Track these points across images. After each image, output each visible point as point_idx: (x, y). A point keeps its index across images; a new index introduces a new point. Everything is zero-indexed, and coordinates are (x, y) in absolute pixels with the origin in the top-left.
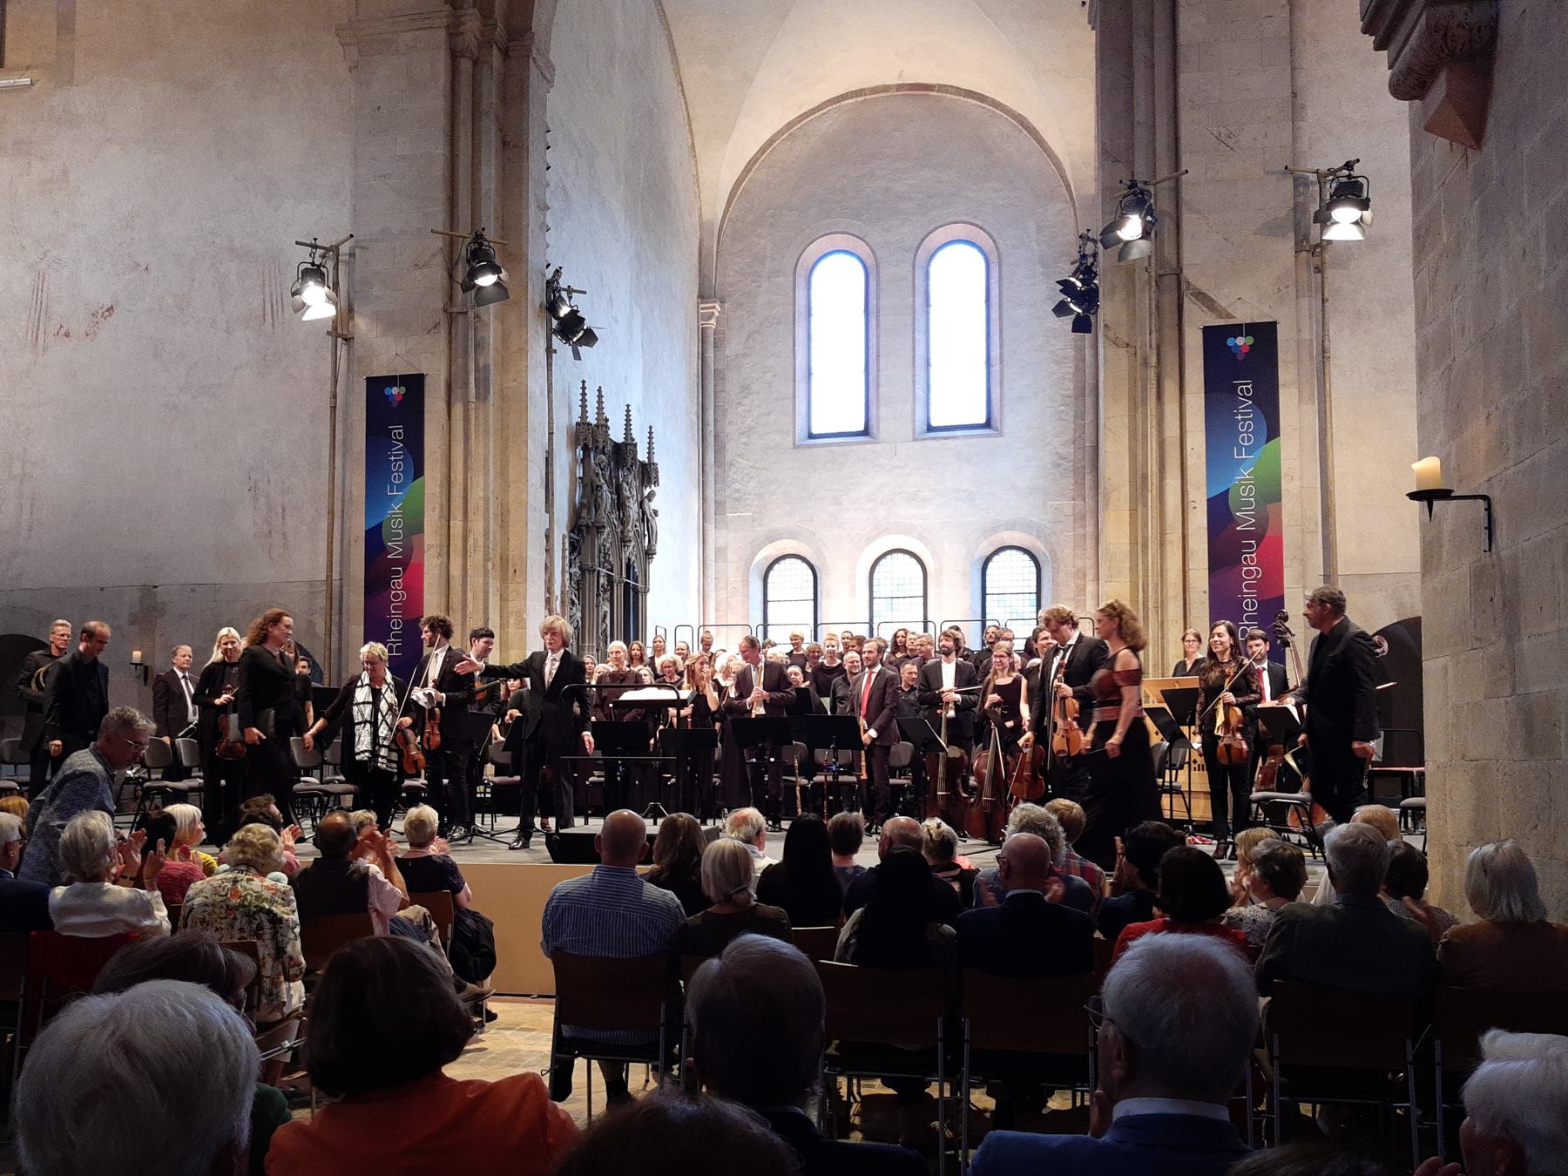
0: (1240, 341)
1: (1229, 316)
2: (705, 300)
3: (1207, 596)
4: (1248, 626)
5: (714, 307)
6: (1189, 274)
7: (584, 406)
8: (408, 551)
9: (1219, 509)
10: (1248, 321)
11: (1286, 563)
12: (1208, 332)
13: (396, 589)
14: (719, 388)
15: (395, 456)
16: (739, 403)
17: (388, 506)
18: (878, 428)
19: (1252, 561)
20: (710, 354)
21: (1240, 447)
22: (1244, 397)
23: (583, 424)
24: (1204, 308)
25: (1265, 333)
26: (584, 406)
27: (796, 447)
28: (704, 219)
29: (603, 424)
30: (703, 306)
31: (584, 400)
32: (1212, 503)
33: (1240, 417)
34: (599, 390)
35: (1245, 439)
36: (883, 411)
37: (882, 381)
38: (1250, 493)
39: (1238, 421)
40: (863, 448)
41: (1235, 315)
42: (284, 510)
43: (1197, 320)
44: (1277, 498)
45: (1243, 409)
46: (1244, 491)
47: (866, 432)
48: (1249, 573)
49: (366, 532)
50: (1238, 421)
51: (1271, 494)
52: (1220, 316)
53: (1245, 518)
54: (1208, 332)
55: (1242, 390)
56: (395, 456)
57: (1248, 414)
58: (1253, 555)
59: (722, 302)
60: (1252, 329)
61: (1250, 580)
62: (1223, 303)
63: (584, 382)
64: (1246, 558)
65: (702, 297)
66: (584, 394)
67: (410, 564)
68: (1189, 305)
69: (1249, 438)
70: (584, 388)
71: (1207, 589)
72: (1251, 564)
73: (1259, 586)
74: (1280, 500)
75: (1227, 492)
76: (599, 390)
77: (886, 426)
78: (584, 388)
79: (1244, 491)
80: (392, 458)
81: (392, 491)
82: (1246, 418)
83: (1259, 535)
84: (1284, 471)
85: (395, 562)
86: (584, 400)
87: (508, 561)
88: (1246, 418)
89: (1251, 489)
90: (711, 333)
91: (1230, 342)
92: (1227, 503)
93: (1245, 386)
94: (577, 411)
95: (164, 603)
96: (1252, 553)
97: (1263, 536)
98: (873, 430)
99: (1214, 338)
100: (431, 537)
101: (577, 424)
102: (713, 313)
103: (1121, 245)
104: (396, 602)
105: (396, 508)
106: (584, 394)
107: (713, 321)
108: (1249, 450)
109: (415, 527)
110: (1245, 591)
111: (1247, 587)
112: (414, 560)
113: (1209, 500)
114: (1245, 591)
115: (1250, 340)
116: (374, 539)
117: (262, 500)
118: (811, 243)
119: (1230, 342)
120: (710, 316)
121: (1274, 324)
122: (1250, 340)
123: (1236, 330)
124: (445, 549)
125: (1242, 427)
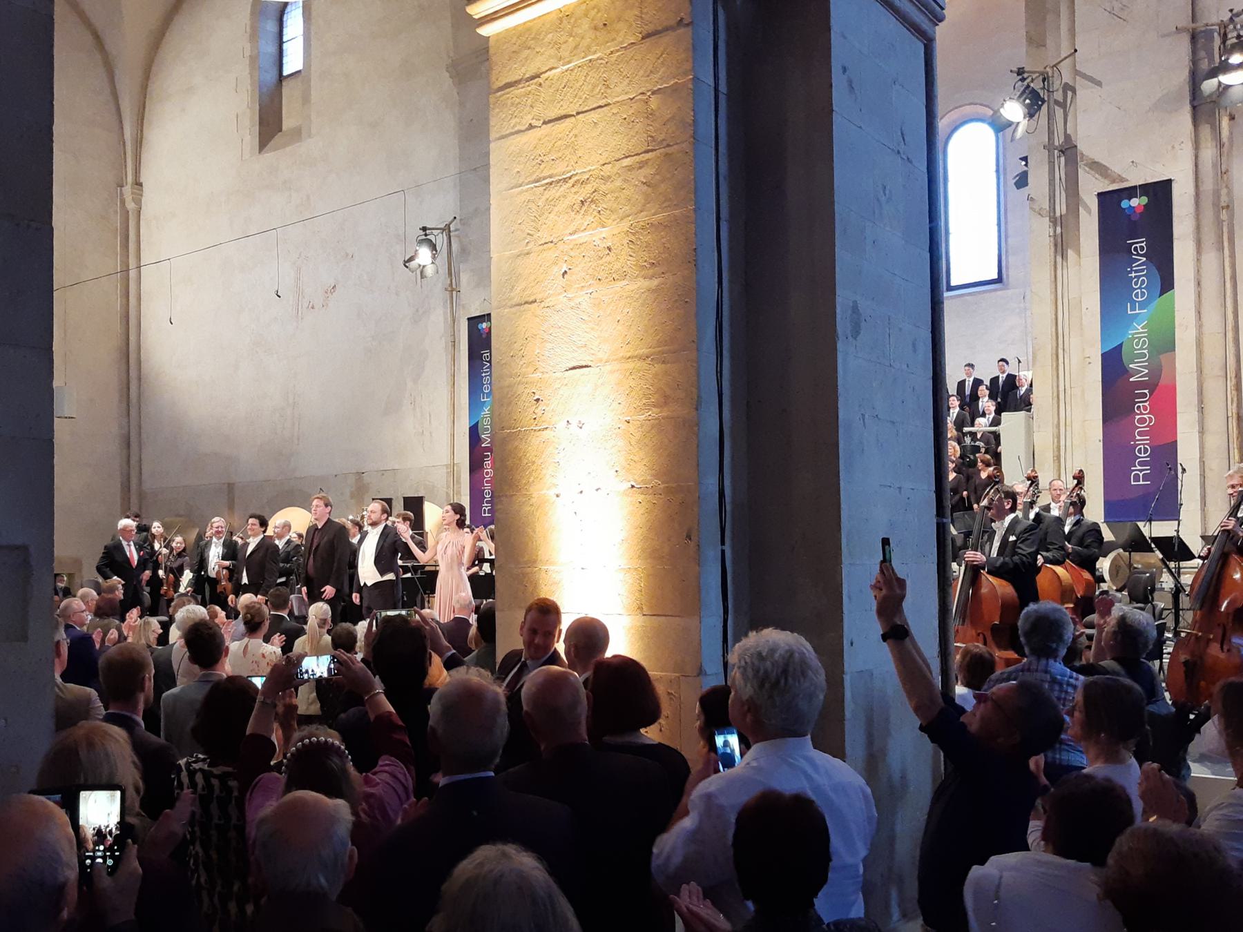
0: (1135, 202)
1: (1122, 180)
3: (1101, 443)
4: (1141, 471)
6: (1082, 147)
9: (1113, 364)
10: (1141, 182)
19: (1146, 410)
21: (1133, 303)
22: (1138, 254)
24: (1097, 176)
25: (1160, 192)
32: (1106, 357)
33: (1133, 275)
37: (1010, 232)
38: (1142, 345)
39: (1132, 278)
40: (997, 295)
42: (430, 416)
43: (1091, 187)
44: (1170, 346)
45: (1135, 267)
47: (999, 280)
48: (1142, 421)
49: (470, 428)
51: (1165, 344)
52: (1113, 181)
53: (1138, 369)
54: (1100, 195)
55: (1136, 249)
56: (485, 372)
57: (1143, 270)
58: (1146, 404)
60: (1146, 189)
61: (1143, 427)
62: (1116, 168)
64: (1139, 407)
68: (1084, 176)
69: (1143, 294)
71: (1101, 439)
72: (1144, 414)
73: (1152, 432)
75: (1122, 343)
77: (1012, 275)
80: (484, 375)
81: (483, 398)
82: (1140, 273)
83: (1152, 385)
85: (487, 449)
88: (1140, 273)
92: (1122, 360)
97: (1157, 385)
99: (1109, 201)
103: (1015, 124)
105: (486, 410)
108: (1143, 305)
110: (1138, 438)
111: (1140, 434)
114: (1138, 438)
115: (1144, 200)
116: (474, 434)
119: (1125, 204)
121: (1169, 182)
122: (1144, 200)
123: (1131, 192)
125: (1136, 284)
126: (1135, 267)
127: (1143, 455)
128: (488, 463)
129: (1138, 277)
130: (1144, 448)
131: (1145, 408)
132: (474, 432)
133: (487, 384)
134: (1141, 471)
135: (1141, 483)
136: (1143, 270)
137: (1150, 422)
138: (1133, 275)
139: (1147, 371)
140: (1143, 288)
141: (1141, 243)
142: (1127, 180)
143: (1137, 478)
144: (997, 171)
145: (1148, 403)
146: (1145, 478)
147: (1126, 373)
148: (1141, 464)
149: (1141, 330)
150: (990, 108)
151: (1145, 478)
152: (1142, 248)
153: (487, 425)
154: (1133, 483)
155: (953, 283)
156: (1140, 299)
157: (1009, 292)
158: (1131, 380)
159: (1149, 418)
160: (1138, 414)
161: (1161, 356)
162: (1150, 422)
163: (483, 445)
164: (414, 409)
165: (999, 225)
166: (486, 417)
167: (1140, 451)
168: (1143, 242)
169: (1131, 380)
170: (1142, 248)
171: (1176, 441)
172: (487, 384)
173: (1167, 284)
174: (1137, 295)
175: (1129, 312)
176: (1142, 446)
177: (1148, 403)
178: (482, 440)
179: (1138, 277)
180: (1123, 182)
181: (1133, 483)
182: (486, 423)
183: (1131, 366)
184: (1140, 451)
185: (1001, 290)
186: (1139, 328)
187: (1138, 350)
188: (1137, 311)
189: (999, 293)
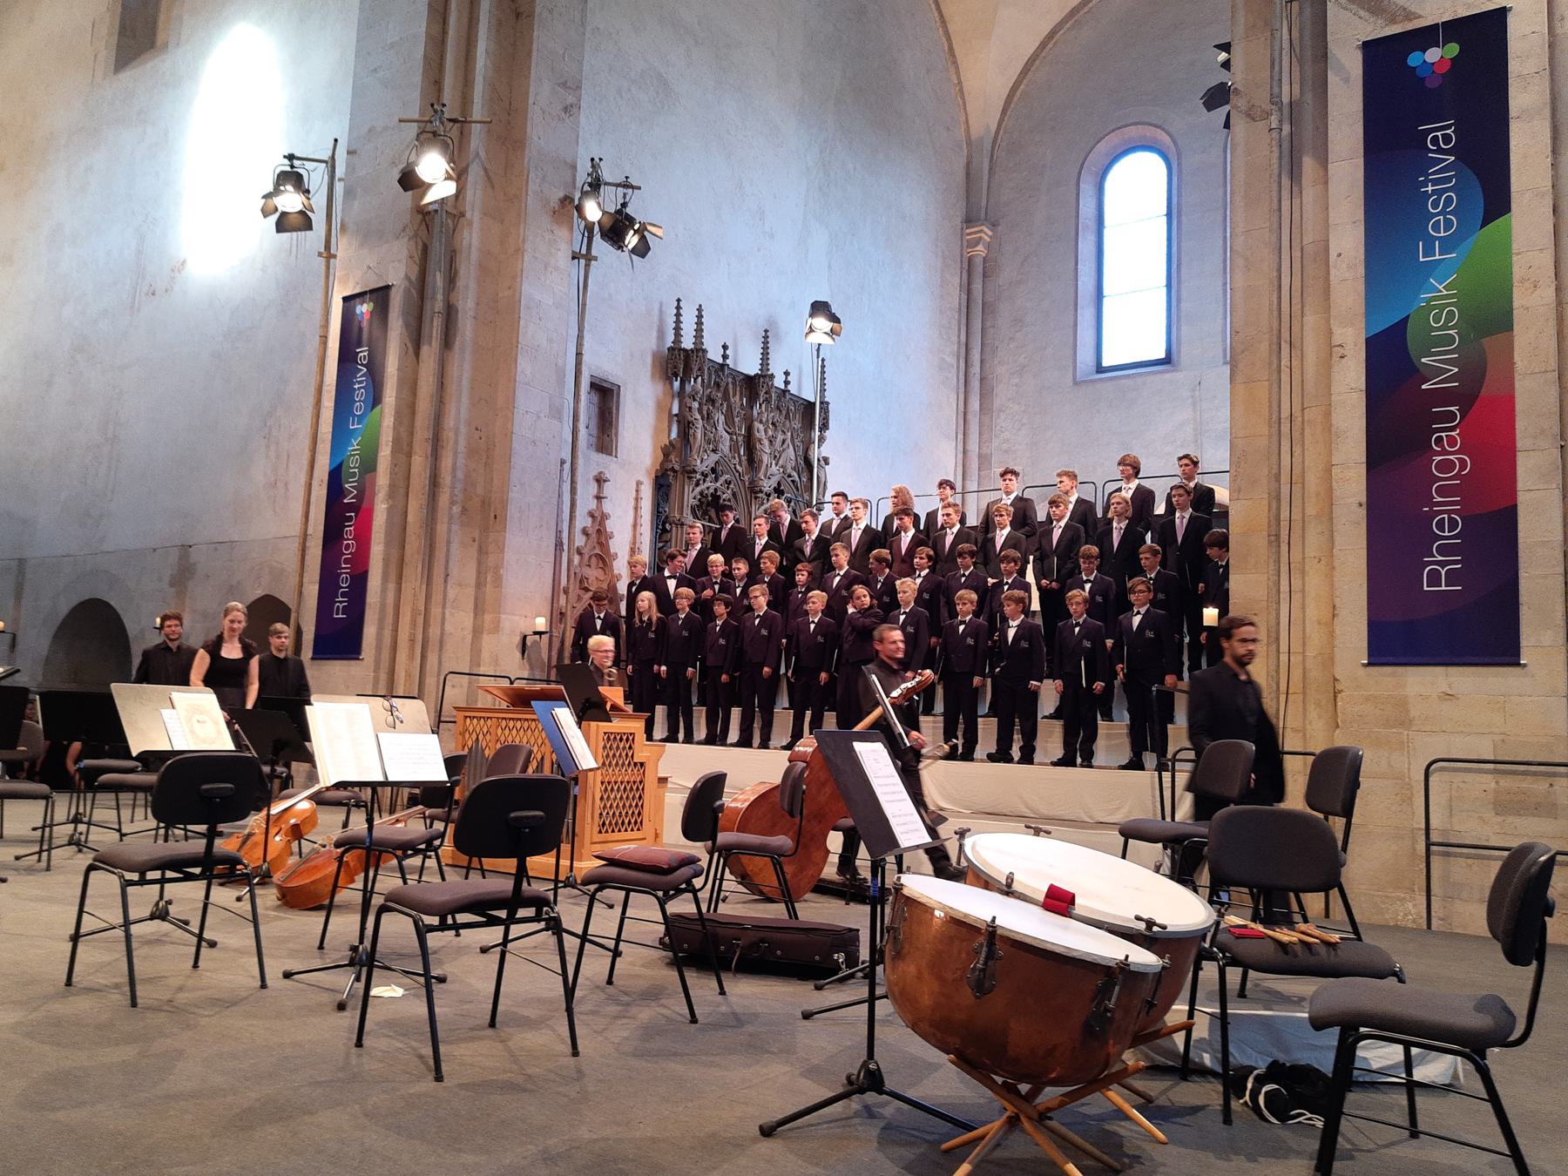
0: (1433, 55)
1: (1409, 16)
2: (973, 224)
3: (1363, 512)
4: (1443, 564)
5: (981, 231)
7: (677, 329)
8: (361, 495)
11: (1522, 442)
12: (1370, 48)
13: (349, 539)
14: (989, 324)
15: (360, 382)
16: (1011, 338)
17: (348, 443)
18: (1179, 352)
19: (1452, 441)
20: (977, 286)
22: (1440, 151)
23: (676, 349)
24: (1362, 13)
26: (677, 329)
27: (1076, 383)
28: (974, 134)
29: (699, 350)
30: (968, 231)
31: (678, 322)
33: (1430, 189)
34: (700, 310)
35: (1441, 218)
36: (1184, 329)
37: (1184, 294)
39: (1427, 195)
41: (1422, 13)
45: (1433, 173)
46: (1437, 320)
47: (1167, 360)
48: (1446, 466)
50: (1427, 195)
52: (1393, 21)
54: (1370, 48)
55: (1435, 140)
56: (360, 382)
57: (1448, 180)
59: (994, 225)
60: (1455, 29)
61: (1447, 479)
63: (679, 300)
64: (1439, 441)
65: (969, 221)
66: (678, 315)
67: (362, 510)
70: (678, 308)
71: (1364, 499)
73: (1466, 488)
74: (1511, 329)
76: (700, 310)
77: (1185, 355)
78: (678, 308)
79: (1437, 319)
80: (356, 386)
84: (1518, 272)
85: (351, 507)
86: (678, 322)
87: (489, 505)
89: (1451, 313)
90: (979, 262)
91: (1414, 59)
93: (1442, 132)
94: (670, 338)
95: (195, 564)
96: (1453, 429)
98: (1174, 357)
100: (382, 479)
101: (669, 349)
102: (981, 238)
104: (347, 555)
106: (678, 315)
107: (980, 247)
109: (369, 466)
112: (365, 505)
113: (1369, 341)
115: (1453, 49)
117: (273, 447)
118: (1098, 142)
119: (1414, 59)
120: (978, 241)
121: (1502, 13)
122: (1453, 49)
123: (1427, 36)
124: (402, 491)
125: (1435, 205)
126: (1433, 173)
127: (1447, 534)
128: (349, 529)
129: (1440, 193)
130: (1450, 518)
131: (1452, 441)
132: (336, 477)
133: (360, 401)
134: (1443, 564)
135: (1443, 588)
136: (1448, 180)
137: (1463, 466)
138: (1430, 189)
139: (1456, 370)
140: (1449, 213)
141: (1442, 132)
142: (1420, 17)
143: (1434, 578)
144: (1169, 215)
145: (1458, 431)
146: (1452, 578)
147: (1416, 374)
148: (1443, 550)
149: (1446, 293)
150: (1163, 129)
151: (1452, 578)
152: (1447, 139)
153: (355, 468)
154: (1426, 589)
155: (1105, 363)
156: (1442, 234)
157: (1178, 376)
158: (1423, 387)
159: (1462, 461)
160: (1439, 454)
161: (1483, 340)
162: (1463, 466)
163: (345, 501)
164: (268, 446)
165: (1169, 285)
166: (354, 455)
167: (1440, 525)
168: (1448, 127)
169: (1423, 387)
170: (1447, 139)
171: (1515, 506)
172: (360, 401)
173: (1497, 202)
174: (1436, 227)
175: (1421, 260)
176: (1446, 516)
177: (1458, 431)
178: (346, 492)
179: (1440, 193)
180: (1410, 20)
181: (1426, 589)
182: (353, 465)
183: (1423, 360)
184: (1440, 525)
185: (1168, 371)
186: (1441, 287)
187: (1439, 329)
188: (1437, 257)
189: (1167, 376)
